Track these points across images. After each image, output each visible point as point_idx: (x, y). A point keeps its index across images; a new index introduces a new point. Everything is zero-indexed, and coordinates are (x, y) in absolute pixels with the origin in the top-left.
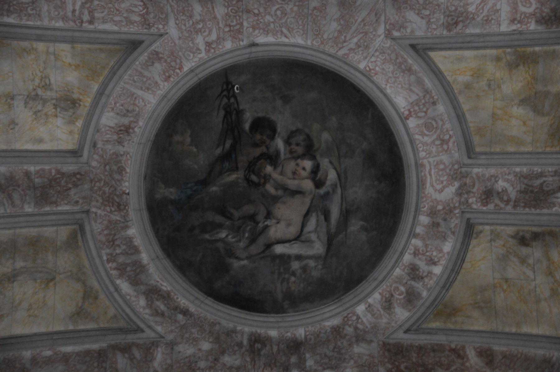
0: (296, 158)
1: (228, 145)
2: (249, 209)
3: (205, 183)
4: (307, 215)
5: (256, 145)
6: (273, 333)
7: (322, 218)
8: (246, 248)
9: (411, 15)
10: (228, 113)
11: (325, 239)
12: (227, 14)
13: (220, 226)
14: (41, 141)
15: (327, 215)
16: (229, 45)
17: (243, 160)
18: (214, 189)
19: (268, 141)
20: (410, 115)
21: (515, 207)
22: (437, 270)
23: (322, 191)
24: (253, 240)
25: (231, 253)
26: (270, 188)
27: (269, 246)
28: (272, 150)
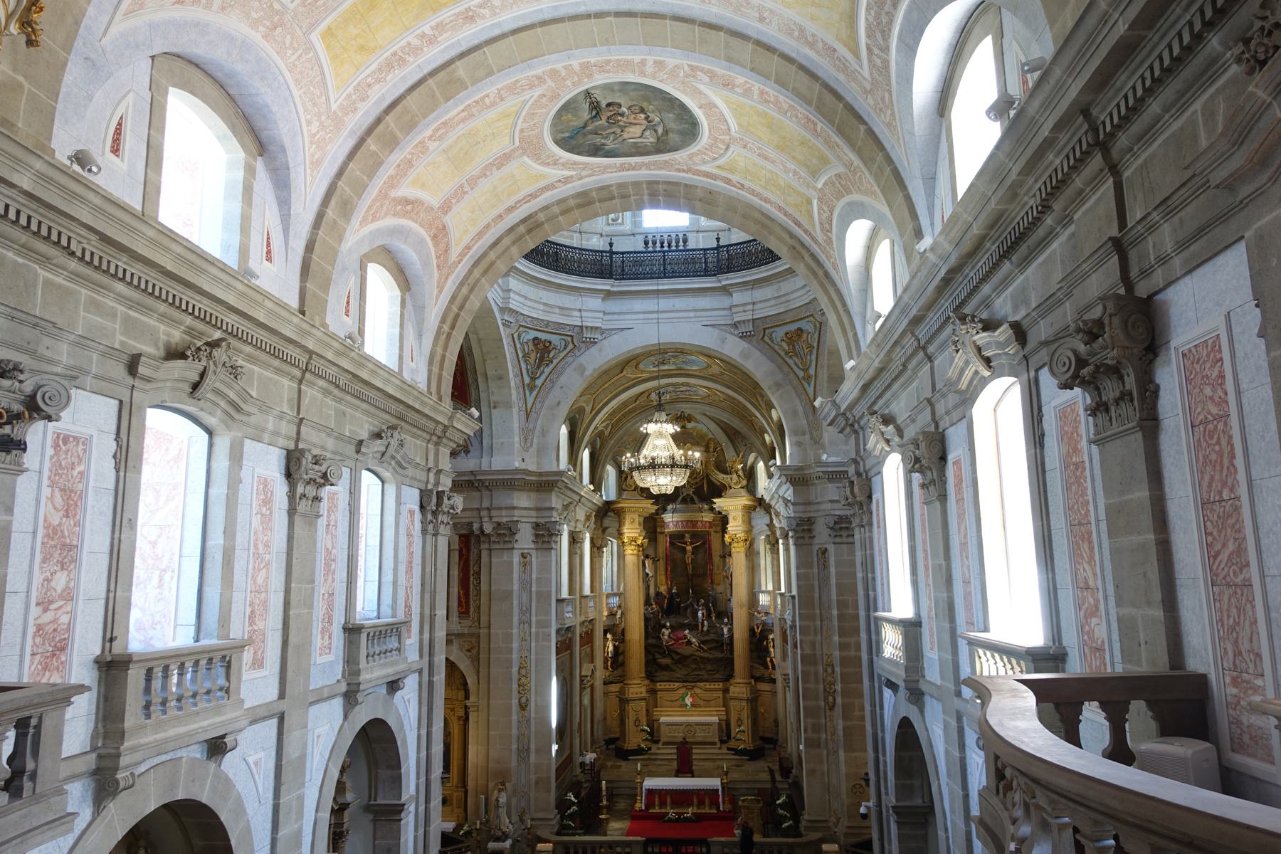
1: (594, 113)
15: (656, 131)
26: (621, 123)
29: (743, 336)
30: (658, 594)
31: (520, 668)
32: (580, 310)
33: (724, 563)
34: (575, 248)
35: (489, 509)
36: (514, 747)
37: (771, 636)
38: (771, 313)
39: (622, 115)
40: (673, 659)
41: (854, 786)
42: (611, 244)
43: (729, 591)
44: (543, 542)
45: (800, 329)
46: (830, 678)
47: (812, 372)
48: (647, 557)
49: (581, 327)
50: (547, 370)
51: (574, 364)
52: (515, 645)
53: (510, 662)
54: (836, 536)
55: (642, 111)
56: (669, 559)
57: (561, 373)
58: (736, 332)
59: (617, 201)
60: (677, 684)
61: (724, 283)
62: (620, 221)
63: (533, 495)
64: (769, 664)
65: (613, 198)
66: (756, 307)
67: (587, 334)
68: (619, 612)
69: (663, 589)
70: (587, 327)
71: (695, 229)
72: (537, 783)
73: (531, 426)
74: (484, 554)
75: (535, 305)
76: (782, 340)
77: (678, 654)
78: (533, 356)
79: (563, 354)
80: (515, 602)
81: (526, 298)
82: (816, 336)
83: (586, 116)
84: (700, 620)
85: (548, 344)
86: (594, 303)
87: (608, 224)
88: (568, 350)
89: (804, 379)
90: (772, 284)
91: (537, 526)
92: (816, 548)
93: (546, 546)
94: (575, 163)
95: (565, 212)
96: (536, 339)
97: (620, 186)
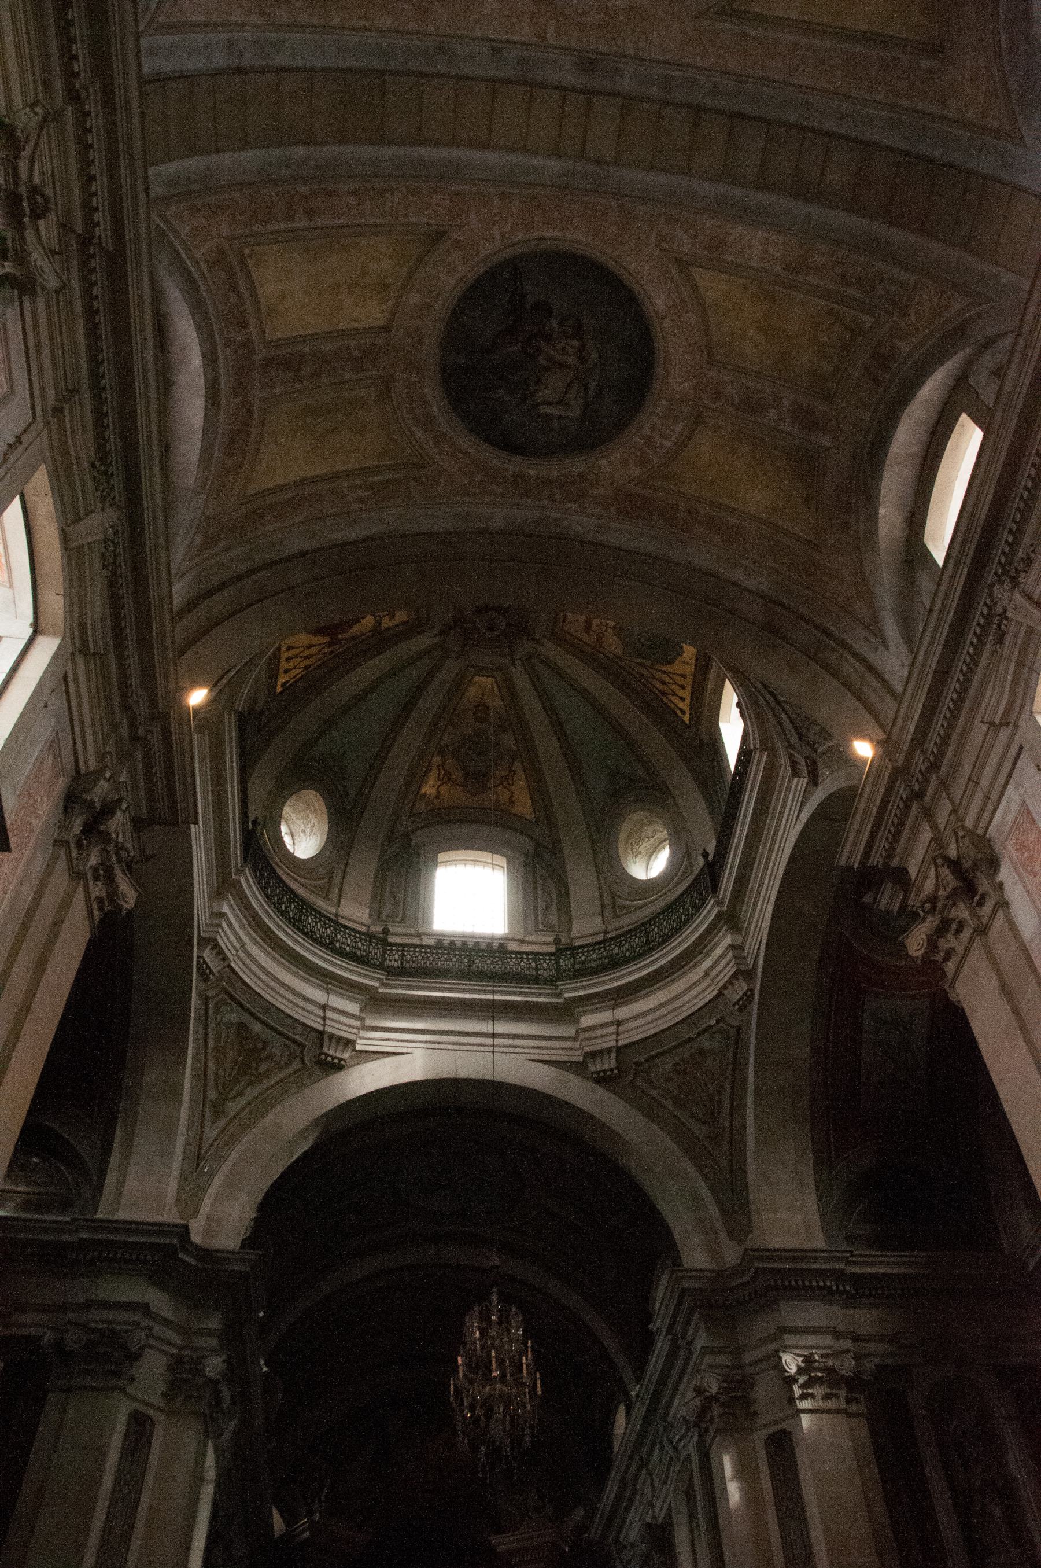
0: (567, 338)
4: (569, 385)
6: (532, 472)
9: (679, 233)
12: (522, 209)
14: (358, 321)
15: (586, 389)
16: (520, 236)
20: (665, 317)
21: (737, 409)
22: (668, 444)
24: (524, 400)
27: (537, 405)
29: (602, 1080)
34: (330, 919)
35: (88, 1305)
45: (702, 1052)
49: (321, 1034)
50: (251, 1093)
55: (579, 331)
66: (621, 1029)
67: (331, 1050)
70: (331, 1036)
78: (231, 1054)
81: (243, 945)
88: (290, 1070)
91: (176, 1364)
92: (765, 1433)
96: (242, 1027)
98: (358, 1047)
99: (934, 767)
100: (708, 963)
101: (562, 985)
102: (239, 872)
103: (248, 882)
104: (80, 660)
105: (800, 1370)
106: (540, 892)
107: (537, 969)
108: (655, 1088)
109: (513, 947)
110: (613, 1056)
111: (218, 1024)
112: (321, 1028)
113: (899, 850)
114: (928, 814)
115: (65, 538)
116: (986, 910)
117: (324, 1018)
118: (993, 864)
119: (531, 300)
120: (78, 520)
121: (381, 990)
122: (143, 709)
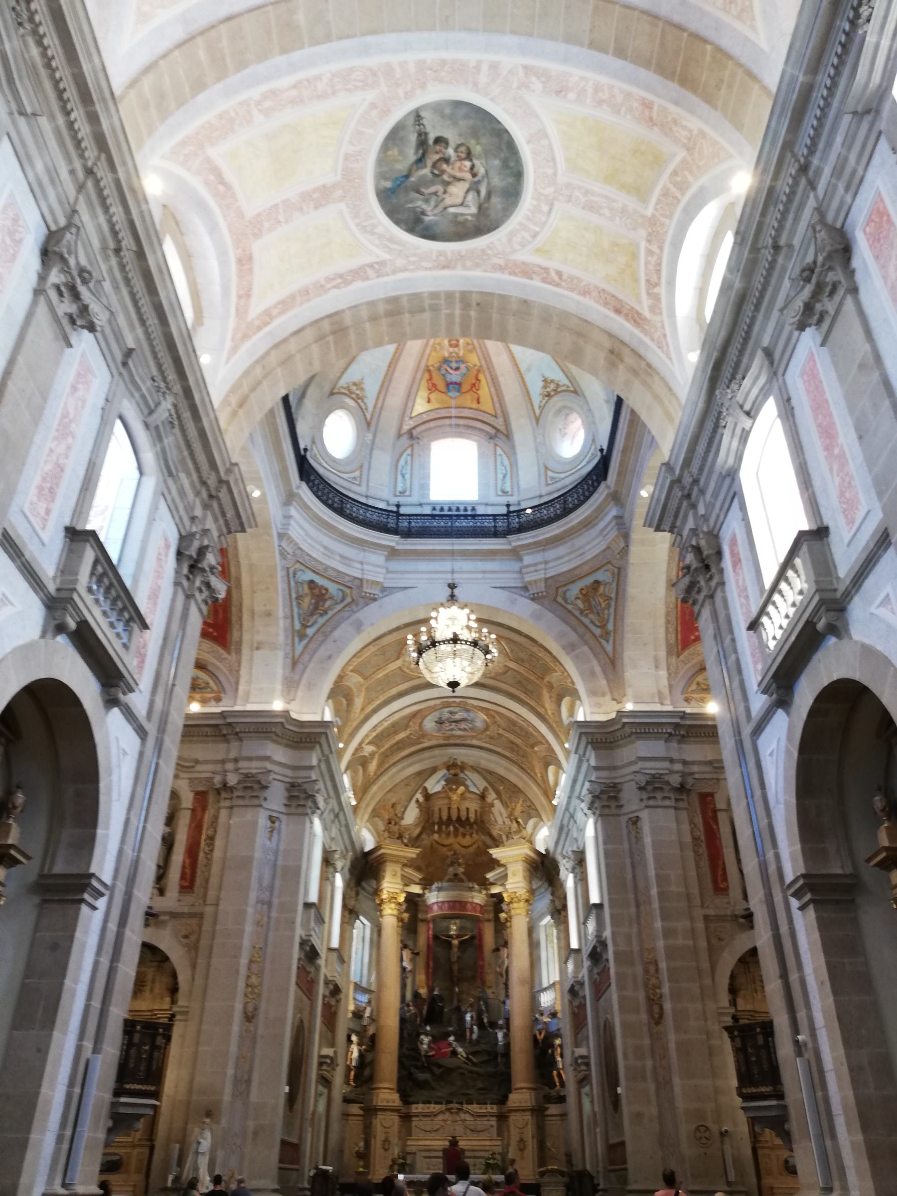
2: (433, 189)
3: (407, 177)
4: (467, 192)
5: (437, 153)
7: (476, 194)
8: (432, 210)
10: (420, 135)
11: (477, 205)
13: (418, 200)
15: (478, 192)
17: (429, 163)
18: (412, 179)
19: (443, 150)
23: (476, 179)
24: (436, 206)
25: (423, 213)
26: (445, 177)
27: (445, 208)
28: (446, 156)
30: (416, 995)
31: (251, 962)
32: (362, 563)
33: (498, 957)
35: (236, 760)
36: (230, 1071)
37: (558, 1042)
38: (564, 570)
39: (447, 160)
40: (433, 1074)
41: (697, 1129)
42: (398, 506)
43: (503, 992)
44: (299, 805)
45: (597, 582)
46: (653, 981)
47: (610, 627)
48: (405, 946)
49: (361, 580)
51: (351, 620)
52: (249, 928)
53: (239, 948)
54: (649, 798)
55: (469, 156)
56: (431, 955)
57: (334, 629)
58: (527, 594)
59: (427, 316)
60: (438, 1107)
61: (514, 544)
62: (407, 493)
63: (290, 752)
64: (556, 1079)
65: (422, 310)
67: (367, 589)
68: (368, 1010)
69: (423, 991)
70: (368, 581)
71: (485, 501)
72: (256, 1134)
73: (296, 677)
74: (224, 813)
75: (317, 546)
76: (577, 598)
77: (439, 1066)
79: (339, 607)
80: (255, 874)
82: (614, 585)
83: (411, 155)
84: (468, 1025)
85: (324, 592)
86: (378, 558)
87: (396, 496)
89: (601, 636)
90: (566, 542)
93: (300, 810)
94: (392, 240)
95: (374, 318)
96: (311, 582)
97: (434, 295)
98: (385, 585)
99: (696, 481)
100: (601, 525)
101: (512, 538)
102: (298, 487)
103: (305, 492)
104: (170, 481)
105: (648, 783)
106: (499, 467)
107: (495, 527)
108: (568, 603)
109: (481, 510)
110: (543, 584)
111: (296, 583)
112: (360, 576)
113: (678, 523)
114: (694, 506)
115: (147, 426)
116: (713, 583)
117: (362, 570)
118: (719, 554)
119: (431, 137)
120: (151, 412)
121: (397, 547)
122: (212, 481)
